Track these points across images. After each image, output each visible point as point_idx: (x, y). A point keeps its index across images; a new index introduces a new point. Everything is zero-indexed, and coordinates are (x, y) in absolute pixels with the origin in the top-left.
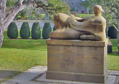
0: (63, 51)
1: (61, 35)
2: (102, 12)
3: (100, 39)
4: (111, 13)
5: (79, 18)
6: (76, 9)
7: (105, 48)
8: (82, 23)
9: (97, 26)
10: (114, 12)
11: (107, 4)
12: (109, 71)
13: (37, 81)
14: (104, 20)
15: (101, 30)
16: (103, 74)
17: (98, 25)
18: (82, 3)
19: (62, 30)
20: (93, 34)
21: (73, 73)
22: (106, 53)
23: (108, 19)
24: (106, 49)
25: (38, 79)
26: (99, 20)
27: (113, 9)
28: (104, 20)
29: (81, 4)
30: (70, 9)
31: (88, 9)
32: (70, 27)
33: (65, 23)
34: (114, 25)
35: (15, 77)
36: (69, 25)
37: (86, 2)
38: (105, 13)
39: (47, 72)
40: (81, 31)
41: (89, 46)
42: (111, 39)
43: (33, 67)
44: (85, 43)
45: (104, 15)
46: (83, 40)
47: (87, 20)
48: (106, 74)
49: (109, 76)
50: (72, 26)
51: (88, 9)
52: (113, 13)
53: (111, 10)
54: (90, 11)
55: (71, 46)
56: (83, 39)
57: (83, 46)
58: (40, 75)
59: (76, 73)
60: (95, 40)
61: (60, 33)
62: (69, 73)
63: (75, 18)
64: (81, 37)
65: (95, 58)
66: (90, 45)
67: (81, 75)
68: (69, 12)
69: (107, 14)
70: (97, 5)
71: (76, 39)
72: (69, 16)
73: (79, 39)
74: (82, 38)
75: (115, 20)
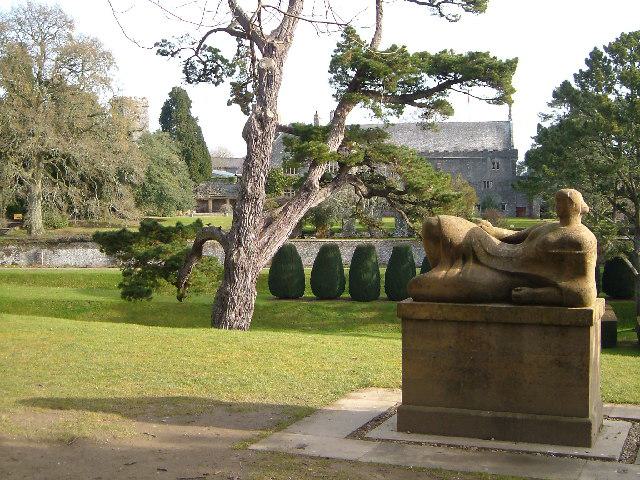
0: (453, 341)
1: (446, 286)
2: (583, 213)
3: (579, 299)
4: (612, 215)
5: (507, 233)
6: (498, 200)
7: (592, 329)
8: (519, 248)
9: (569, 256)
10: (623, 211)
11: (601, 185)
12: (606, 405)
13: (368, 439)
14: (588, 237)
15: (580, 270)
16: (587, 415)
17: (571, 254)
18: (519, 182)
19: (451, 270)
20: (555, 286)
21: (488, 413)
22: (596, 349)
23: (605, 234)
24: (596, 334)
25: (373, 433)
26: (574, 235)
27: (619, 201)
28: (588, 237)
29: (516, 184)
30: (476, 200)
31: (537, 203)
32: (477, 261)
33: (460, 245)
34: (622, 255)
35: (294, 426)
36: (474, 253)
37: (529, 178)
38: (595, 214)
39: (400, 411)
40: (513, 275)
41: (541, 324)
42: (612, 302)
43: (353, 394)
44: (529, 313)
45: (590, 221)
46: (523, 304)
47: (533, 238)
48: (596, 415)
49: (605, 422)
50: (483, 259)
51: (537, 203)
52: (620, 217)
53: (613, 203)
54: (543, 209)
55: (483, 322)
56: (519, 301)
57: (521, 325)
58: (379, 419)
59: (499, 414)
60: (560, 304)
61: (445, 282)
62: (473, 413)
63: (495, 232)
64: (514, 292)
65: (560, 364)
66: (545, 321)
67: (515, 420)
68: (473, 210)
69: (601, 218)
70: (565, 188)
71: (498, 302)
72: (475, 226)
73: (508, 299)
74: (517, 297)
75: (626, 238)
